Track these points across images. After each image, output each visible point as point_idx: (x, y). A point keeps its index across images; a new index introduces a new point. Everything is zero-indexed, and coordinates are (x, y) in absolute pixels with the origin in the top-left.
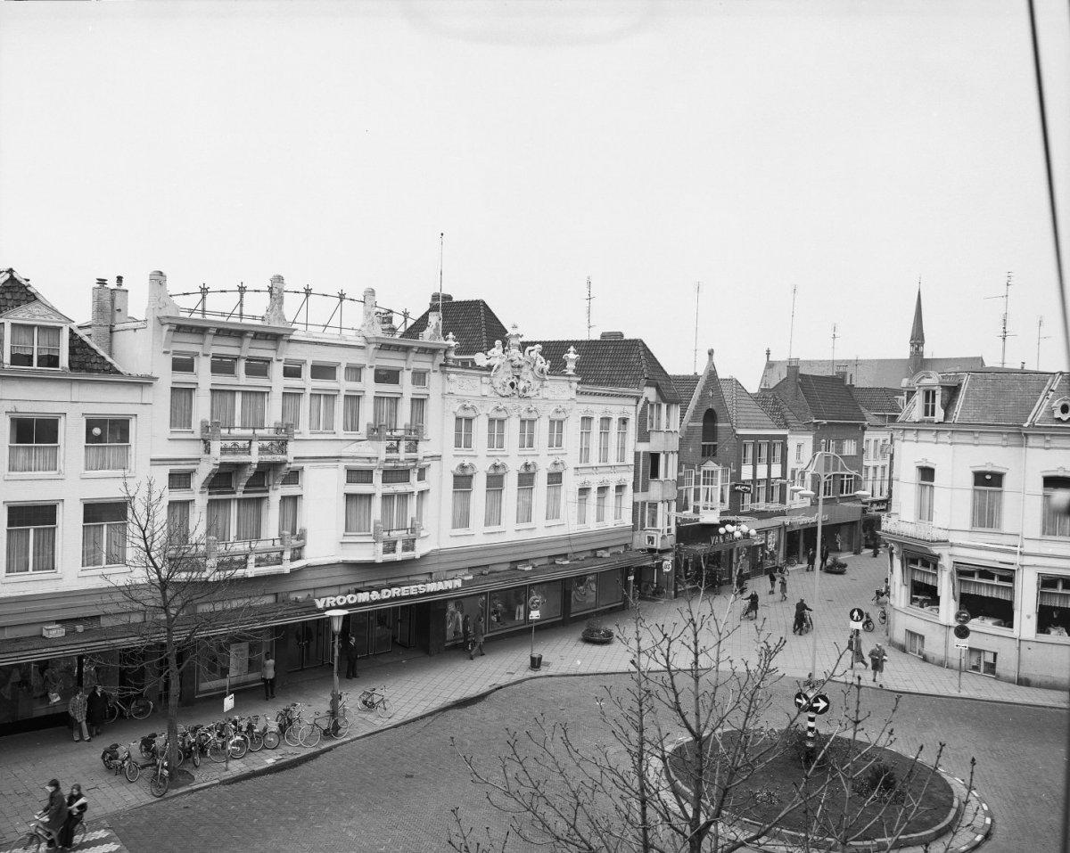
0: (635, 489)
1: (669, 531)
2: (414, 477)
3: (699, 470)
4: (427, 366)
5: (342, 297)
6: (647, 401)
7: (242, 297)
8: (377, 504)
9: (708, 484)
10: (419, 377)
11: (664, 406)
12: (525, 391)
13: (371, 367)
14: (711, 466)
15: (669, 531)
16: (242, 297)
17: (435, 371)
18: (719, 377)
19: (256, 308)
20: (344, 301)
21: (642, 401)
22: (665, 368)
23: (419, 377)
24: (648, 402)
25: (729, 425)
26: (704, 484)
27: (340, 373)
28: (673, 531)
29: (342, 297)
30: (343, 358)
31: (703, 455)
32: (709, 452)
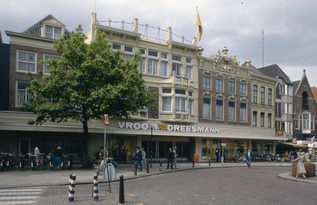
0: (276, 116)
1: (290, 133)
2: (187, 93)
3: (302, 114)
4: (192, 56)
5: (159, 29)
6: (279, 84)
7: (123, 24)
8: (173, 101)
9: (305, 119)
10: (188, 60)
11: (286, 86)
12: (230, 70)
13: (170, 53)
14: (306, 112)
15: (290, 133)
16: (123, 24)
17: (195, 58)
18: (311, 87)
19: (130, 29)
20: (160, 30)
21: (277, 84)
22: (286, 74)
23: (188, 60)
24: (280, 84)
25: (313, 99)
26: (304, 119)
27: (159, 54)
28: (292, 134)
29: (159, 29)
30: (160, 50)
31: (303, 108)
32: (305, 107)
